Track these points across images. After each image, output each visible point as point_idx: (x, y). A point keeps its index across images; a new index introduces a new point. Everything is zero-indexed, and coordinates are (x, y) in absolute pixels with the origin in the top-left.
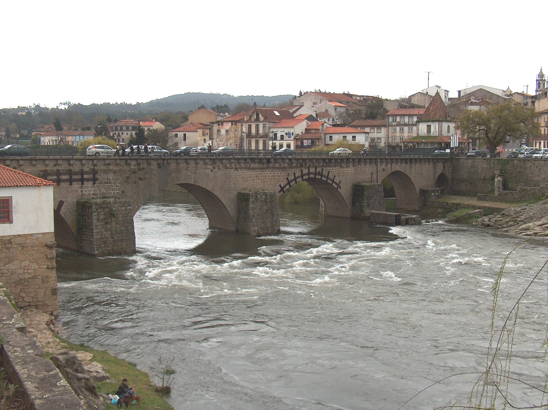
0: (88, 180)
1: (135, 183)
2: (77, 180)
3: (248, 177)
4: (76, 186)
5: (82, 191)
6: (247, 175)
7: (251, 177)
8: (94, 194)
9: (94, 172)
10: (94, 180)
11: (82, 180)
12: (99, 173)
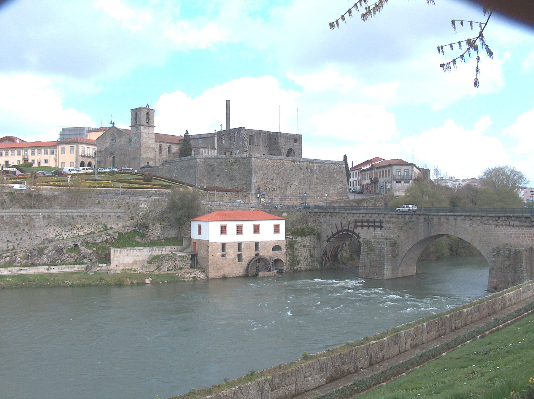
0: (377, 227)
1: (407, 231)
2: (372, 226)
3: (511, 234)
4: (371, 229)
5: (375, 234)
6: (510, 231)
7: (515, 234)
8: (381, 236)
9: (381, 222)
10: (381, 227)
11: (374, 227)
12: (384, 222)
